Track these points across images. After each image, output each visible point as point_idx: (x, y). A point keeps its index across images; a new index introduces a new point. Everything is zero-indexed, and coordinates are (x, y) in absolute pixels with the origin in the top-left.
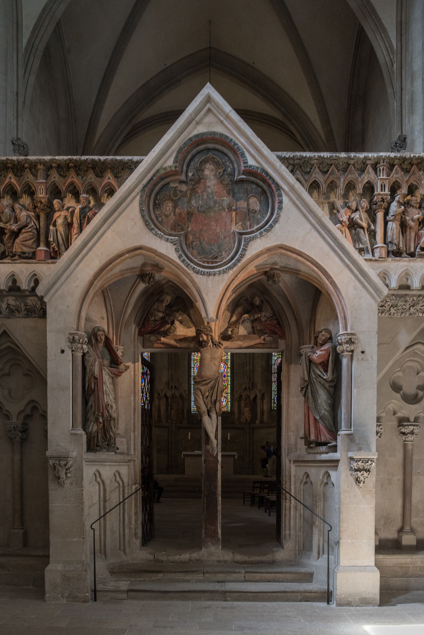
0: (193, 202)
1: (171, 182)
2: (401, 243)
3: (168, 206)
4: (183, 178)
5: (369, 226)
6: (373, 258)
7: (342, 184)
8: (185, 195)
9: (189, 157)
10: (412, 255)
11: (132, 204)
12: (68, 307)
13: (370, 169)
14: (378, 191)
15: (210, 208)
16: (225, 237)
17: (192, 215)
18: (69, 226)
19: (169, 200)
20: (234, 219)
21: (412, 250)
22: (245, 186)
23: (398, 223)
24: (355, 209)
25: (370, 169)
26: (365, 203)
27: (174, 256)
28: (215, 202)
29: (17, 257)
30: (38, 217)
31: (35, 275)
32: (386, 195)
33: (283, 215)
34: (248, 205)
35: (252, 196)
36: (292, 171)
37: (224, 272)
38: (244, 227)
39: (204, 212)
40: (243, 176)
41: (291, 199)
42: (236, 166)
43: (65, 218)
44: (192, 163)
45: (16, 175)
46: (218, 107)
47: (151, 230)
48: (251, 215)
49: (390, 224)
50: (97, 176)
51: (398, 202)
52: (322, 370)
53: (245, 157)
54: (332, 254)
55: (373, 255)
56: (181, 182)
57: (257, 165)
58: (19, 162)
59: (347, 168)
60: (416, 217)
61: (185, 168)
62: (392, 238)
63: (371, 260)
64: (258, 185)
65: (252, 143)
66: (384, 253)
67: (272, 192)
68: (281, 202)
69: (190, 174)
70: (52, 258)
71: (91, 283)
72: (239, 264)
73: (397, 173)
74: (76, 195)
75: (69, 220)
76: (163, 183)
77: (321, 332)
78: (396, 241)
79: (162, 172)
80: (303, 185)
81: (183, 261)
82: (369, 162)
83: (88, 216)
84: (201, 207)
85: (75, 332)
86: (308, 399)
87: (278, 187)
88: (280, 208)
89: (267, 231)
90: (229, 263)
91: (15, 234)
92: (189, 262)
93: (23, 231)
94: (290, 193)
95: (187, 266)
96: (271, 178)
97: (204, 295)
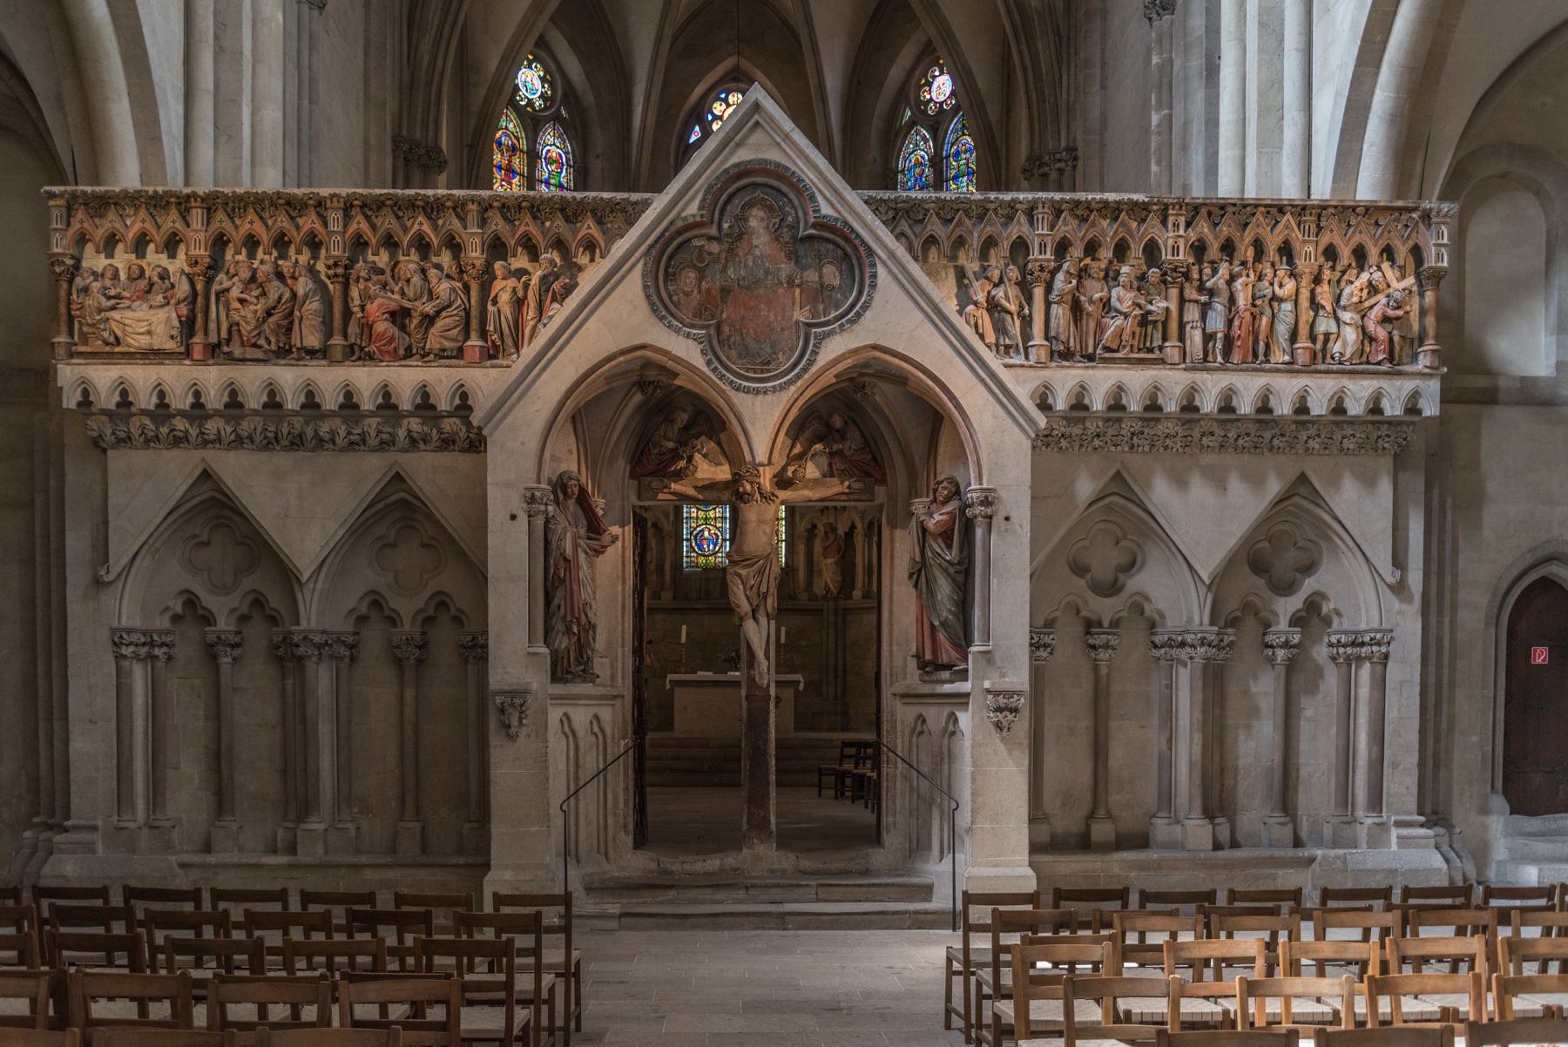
0: (730, 271)
1: (694, 237)
2: (1072, 340)
3: (690, 276)
4: (713, 231)
5: (1021, 307)
6: (1026, 363)
7: (975, 241)
8: (716, 259)
9: (724, 197)
10: (1091, 358)
11: (629, 276)
12: (523, 444)
14: (1035, 254)
15: (757, 282)
16: (783, 330)
17: (729, 292)
18: (519, 303)
19: (689, 267)
21: (1090, 350)
23: (1067, 307)
24: (996, 280)
26: (1013, 273)
27: (699, 362)
28: (767, 272)
30: (467, 288)
31: (462, 385)
32: (1048, 260)
33: (877, 296)
34: (821, 277)
36: (891, 223)
37: (782, 388)
39: (748, 288)
40: (812, 231)
43: (514, 291)
45: (429, 218)
46: (772, 120)
47: (662, 318)
48: (826, 293)
49: (1054, 306)
50: (567, 220)
51: (1068, 272)
52: (943, 545)
53: (816, 201)
54: (957, 360)
55: (1027, 358)
56: (710, 238)
57: (835, 215)
58: (437, 199)
59: (985, 214)
60: (1097, 296)
61: (716, 216)
62: (1058, 333)
63: (1022, 366)
64: (837, 245)
65: (826, 181)
66: (1043, 355)
67: (859, 258)
68: (874, 276)
69: (725, 226)
70: (491, 357)
71: (561, 405)
72: (806, 376)
73: (1066, 225)
74: (534, 254)
76: (679, 240)
78: (1063, 338)
79: (680, 224)
80: (910, 249)
81: (714, 370)
84: (744, 279)
85: (534, 485)
86: (921, 593)
87: (871, 252)
88: (873, 286)
89: (852, 322)
91: (429, 320)
92: (724, 372)
93: (444, 314)
94: (889, 263)
95: (721, 379)
96: (858, 236)
97: (749, 426)
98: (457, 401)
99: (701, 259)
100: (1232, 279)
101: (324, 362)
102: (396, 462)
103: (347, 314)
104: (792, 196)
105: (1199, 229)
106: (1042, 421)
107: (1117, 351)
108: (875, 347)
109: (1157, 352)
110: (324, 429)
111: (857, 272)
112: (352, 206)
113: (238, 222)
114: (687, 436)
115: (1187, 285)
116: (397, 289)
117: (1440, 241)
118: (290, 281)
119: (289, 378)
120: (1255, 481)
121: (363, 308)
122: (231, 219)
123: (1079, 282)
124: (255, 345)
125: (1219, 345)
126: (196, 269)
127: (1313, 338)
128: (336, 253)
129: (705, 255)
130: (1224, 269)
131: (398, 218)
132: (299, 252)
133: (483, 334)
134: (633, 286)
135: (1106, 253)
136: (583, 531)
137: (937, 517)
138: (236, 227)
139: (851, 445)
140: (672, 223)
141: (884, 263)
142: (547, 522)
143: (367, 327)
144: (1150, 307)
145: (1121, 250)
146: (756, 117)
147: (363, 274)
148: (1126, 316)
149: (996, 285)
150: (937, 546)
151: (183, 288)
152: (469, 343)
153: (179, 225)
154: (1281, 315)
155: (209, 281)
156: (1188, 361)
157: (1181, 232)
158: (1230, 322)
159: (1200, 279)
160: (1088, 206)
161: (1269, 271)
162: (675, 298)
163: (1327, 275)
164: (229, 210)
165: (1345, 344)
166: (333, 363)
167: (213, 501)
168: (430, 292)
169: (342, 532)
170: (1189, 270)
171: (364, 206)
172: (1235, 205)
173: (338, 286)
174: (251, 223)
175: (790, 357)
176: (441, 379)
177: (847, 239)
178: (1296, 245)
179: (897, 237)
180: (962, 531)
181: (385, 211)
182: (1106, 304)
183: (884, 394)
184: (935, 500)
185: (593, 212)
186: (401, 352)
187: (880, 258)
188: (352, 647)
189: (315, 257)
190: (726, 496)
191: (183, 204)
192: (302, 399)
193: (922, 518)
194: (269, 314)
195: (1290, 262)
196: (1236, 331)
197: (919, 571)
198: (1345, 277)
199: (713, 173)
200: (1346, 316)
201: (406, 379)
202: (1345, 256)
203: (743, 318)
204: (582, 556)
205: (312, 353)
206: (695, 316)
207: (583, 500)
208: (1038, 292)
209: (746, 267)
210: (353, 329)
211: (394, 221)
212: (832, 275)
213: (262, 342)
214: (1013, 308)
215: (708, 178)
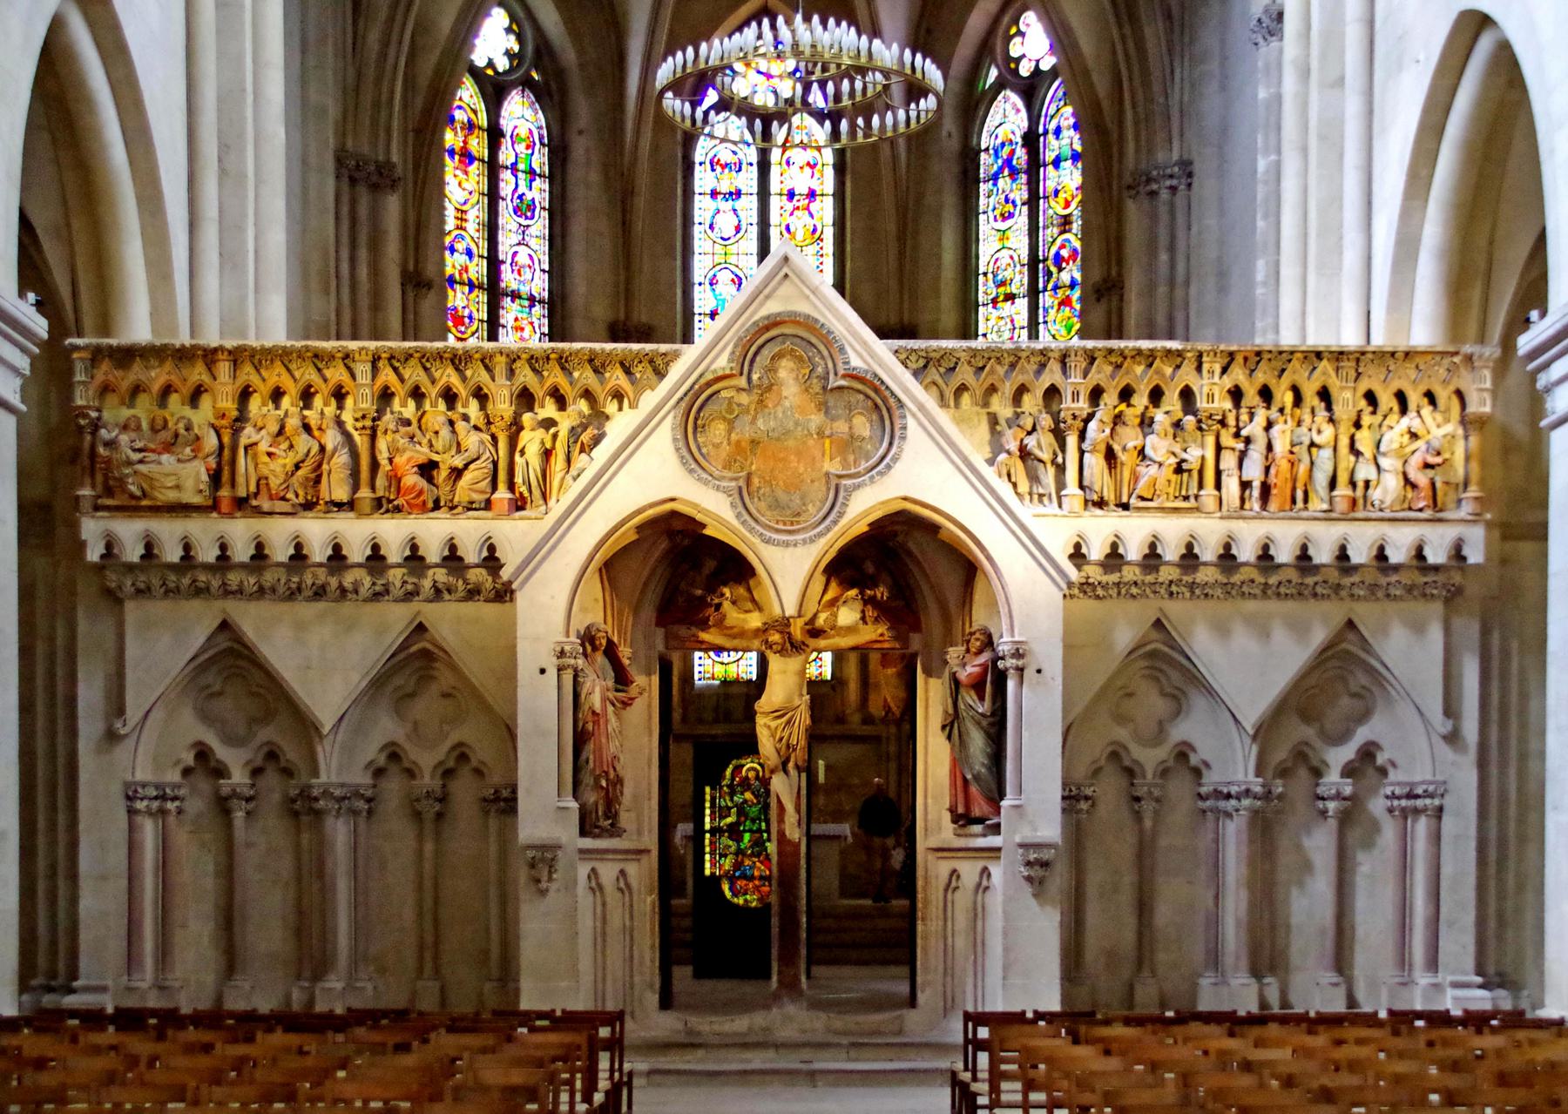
0: (760, 423)
3: (718, 430)
7: (1008, 388)
9: (753, 349)
10: (1126, 507)
13: (1054, 366)
15: (787, 433)
16: (812, 481)
17: (758, 443)
18: (547, 454)
20: (828, 452)
21: (1125, 499)
22: (846, 395)
25: (1054, 366)
26: (1046, 421)
28: (797, 424)
29: (460, 509)
32: (1081, 409)
34: (850, 428)
35: (859, 413)
38: (845, 464)
39: (778, 439)
41: (921, 424)
42: (830, 365)
43: (543, 443)
44: (758, 359)
45: (457, 369)
50: (596, 371)
52: (975, 697)
53: (846, 353)
55: (1060, 506)
57: (865, 367)
60: (1130, 445)
62: (1092, 483)
64: (868, 397)
68: (904, 428)
69: (755, 377)
71: (591, 558)
72: (836, 528)
75: (548, 446)
77: (974, 633)
79: (709, 376)
82: (1050, 354)
83: (582, 443)
87: (901, 404)
88: (903, 438)
89: (881, 474)
90: (820, 523)
91: (457, 473)
93: (472, 467)
94: (920, 415)
98: (485, 554)
99: (730, 411)
100: (1269, 425)
101: (351, 515)
102: (418, 613)
103: (375, 465)
104: (822, 348)
105: (1233, 376)
106: (1073, 574)
107: (1151, 500)
108: (905, 499)
109: (1192, 499)
110: (348, 579)
111: (887, 423)
112: (379, 358)
113: (264, 373)
114: (714, 584)
115: (1223, 432)
116: (425, 441)
117: (1483, 386)
118: (316, 433)
119: (317, 532)
120: (1299, 629)
121: (391, 460)
122: (258, 371)
123: (1113, 430)
124: (283, 499)
125: (1256, 493)
126: (224, 422)
127: (1353, 484)
128: (364, 406)
129: (735, 406)
130: (1261, 416)
131: (426, 369)
132: (326, 404)
133: (511, 486)
134: (663, 439)
135: (1141, 400)
136: (611, 683)
137: (969, 669)
138: (264, 380)
139: (881, 592)
140: (701, 376)
141: (914, 415)
142: (576, 677)
143: (395, 479)
144: (1185, 456)
145: (1156, 396)
146: (785, 270)
147: (392, 426)
148: (1160, 465)
149: (1029, 433)
150: (969, 697)
151: (211, 442)
152: (495, 496)
153: (206, 378)
154: (1318, 462)
155: (236, 432)
156: (1225, 508)
157: (1216, 379)
158: (1267, 469)
159: (1237, 426)
160: (1122, 353)
161: (1307, 418)
162: (704, 450)
163: (1366, 420)
164: (256, 362)
165: (1385, 491)
166: (361, 515)
167: (229, 652)
168: (459, 444)
169: (364, 684)
170: (1224, 416)
171: (391, 358)
172: (1270, 352)
173: (366, 439)
174: (279, 375)
175: (821, 509)
176: (469, 532)
177: (876, 390)
178: (1334, 392)
179: (926, 388)
180: (994, 682)
181: (413, 362)
182: (1141, 452)
183: (916, 544)
184: (968, 651)
185: (622, 364)
186: (430, 505)
187: (910, 410)
188: (369, 800)
189: (340, 407)
190: (756, 643)
191: (210, 356)
192: (329, 552)
193: (955, 669)
194: (297, 467)
195: (1329, 408)
196: (1272, 480)
197: (952, 724)
198: (1386, 422)
199: (743, 325)
200: (1384, 462)
201: (433, 532)
202: (1387, 400)
203: (772, 471)
204: (610, 709)
205: (340, 506)
206: (724, 468)
207: (611, 652)
208: (1072, 441)
209: (775, 417)
210: (381, 482)
211: (422, 373)
212: (863, 425)
213: (290, 495)
214: (1046, 456)
215: (738, 331)
